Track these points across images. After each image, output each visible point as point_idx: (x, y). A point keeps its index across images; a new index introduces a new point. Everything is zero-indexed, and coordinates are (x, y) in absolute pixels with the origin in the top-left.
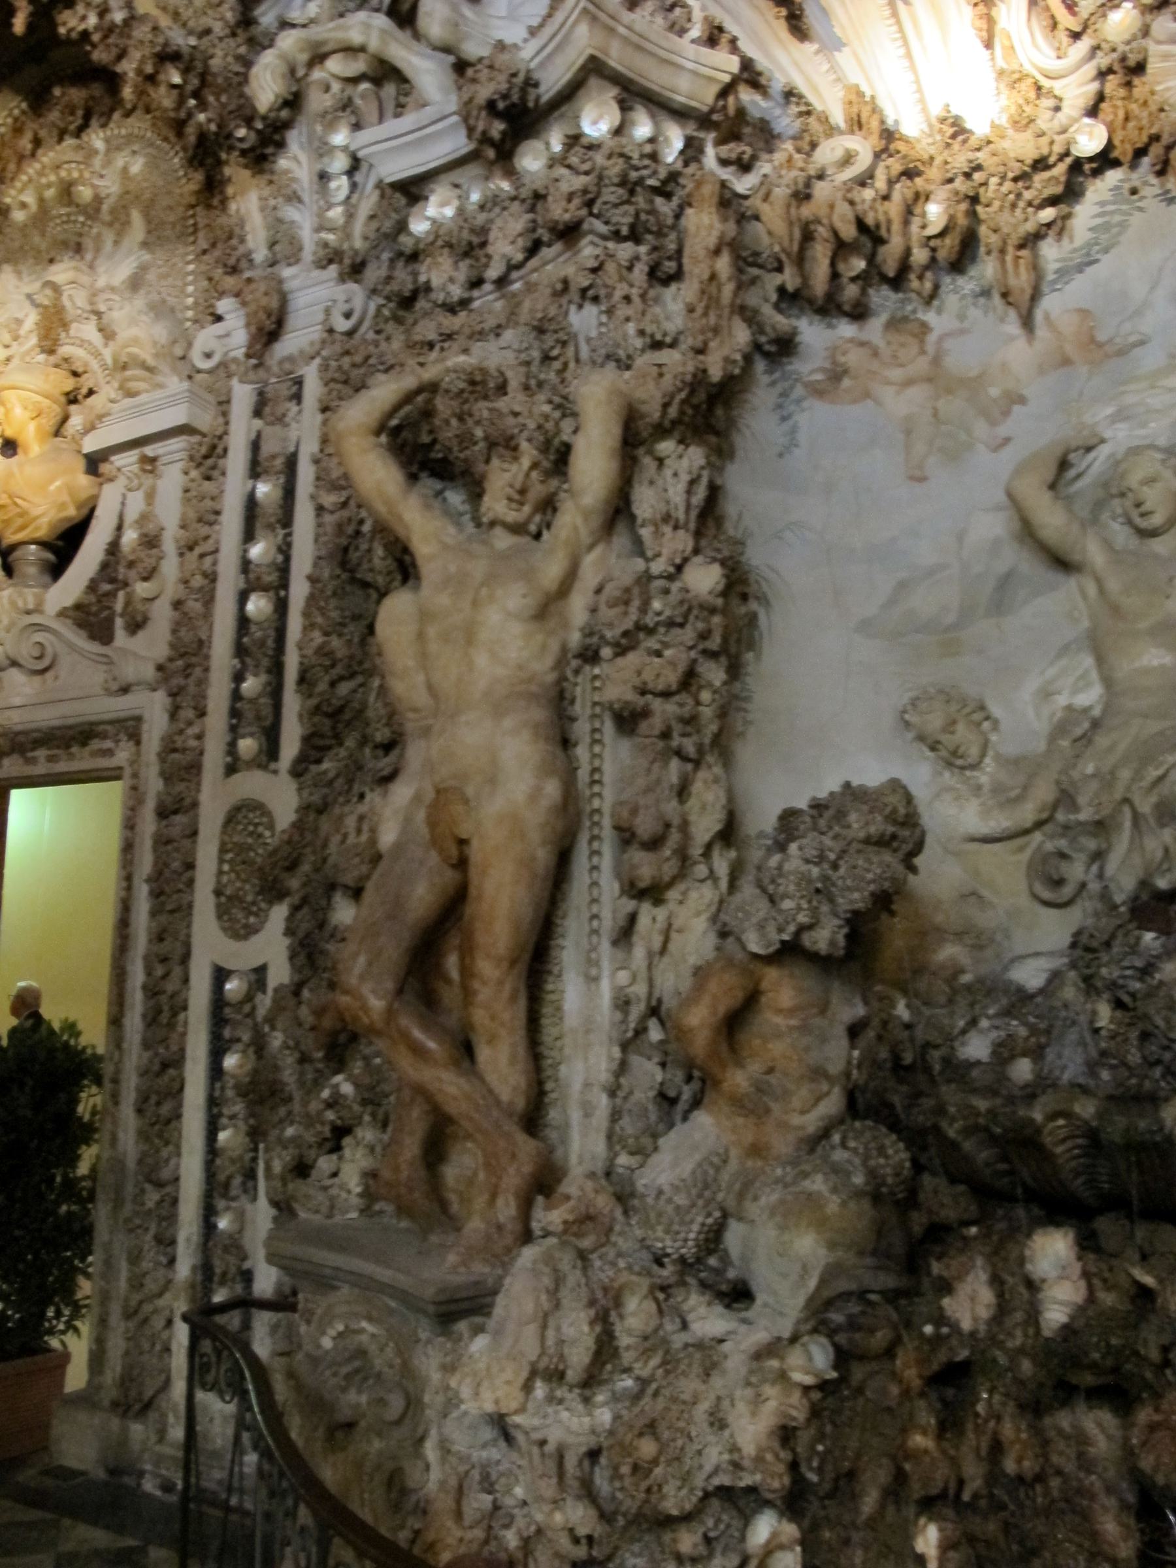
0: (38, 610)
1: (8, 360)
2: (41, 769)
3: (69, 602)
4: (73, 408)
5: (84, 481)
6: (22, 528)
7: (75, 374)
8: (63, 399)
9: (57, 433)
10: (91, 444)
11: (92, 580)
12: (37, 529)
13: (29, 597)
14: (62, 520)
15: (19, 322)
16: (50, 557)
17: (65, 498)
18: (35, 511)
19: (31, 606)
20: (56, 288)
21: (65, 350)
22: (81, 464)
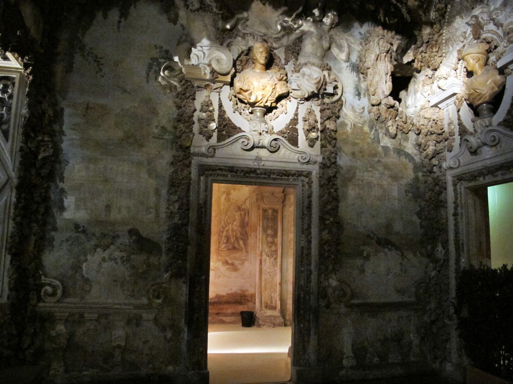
0: (491, 125)
1: (464, 46)
2: (499, 178)
3: (501, 120)
4: (490, 54)
5: (498, 77)
6: (480, 99)
7: (489, 43)
8: (486, 53)
9: (486, 64)
10: (499, 65)
11: (508, 111)
12: (485, 98)
13: (487, 121)
14: (493, 93)
15: (465, 33)
16: (492, 106)
17: (493, 85)
18: (483, 93)
19: (488, 124)
20: (476, 17)
21: (483, 36)
22: (497, 72)
